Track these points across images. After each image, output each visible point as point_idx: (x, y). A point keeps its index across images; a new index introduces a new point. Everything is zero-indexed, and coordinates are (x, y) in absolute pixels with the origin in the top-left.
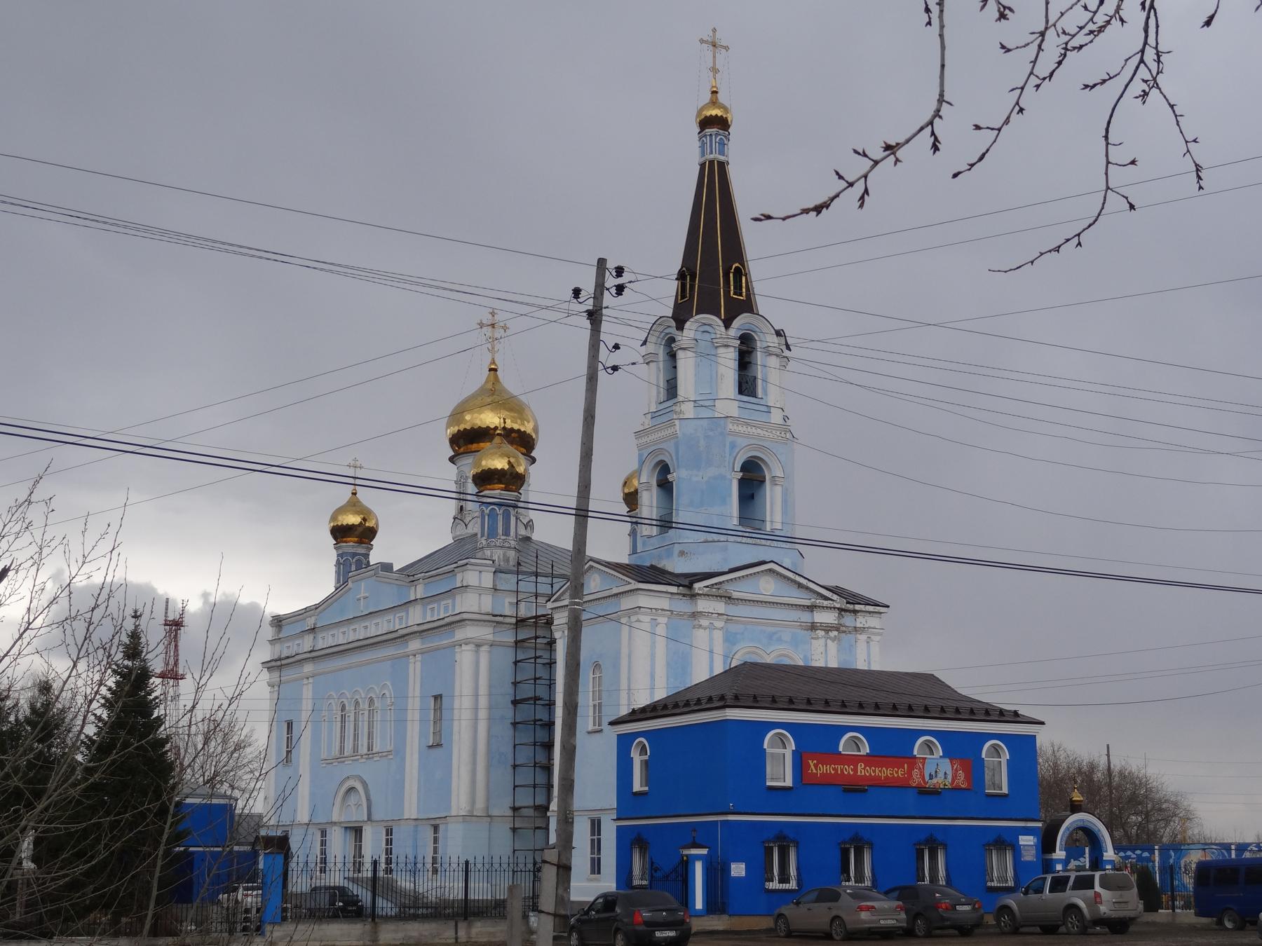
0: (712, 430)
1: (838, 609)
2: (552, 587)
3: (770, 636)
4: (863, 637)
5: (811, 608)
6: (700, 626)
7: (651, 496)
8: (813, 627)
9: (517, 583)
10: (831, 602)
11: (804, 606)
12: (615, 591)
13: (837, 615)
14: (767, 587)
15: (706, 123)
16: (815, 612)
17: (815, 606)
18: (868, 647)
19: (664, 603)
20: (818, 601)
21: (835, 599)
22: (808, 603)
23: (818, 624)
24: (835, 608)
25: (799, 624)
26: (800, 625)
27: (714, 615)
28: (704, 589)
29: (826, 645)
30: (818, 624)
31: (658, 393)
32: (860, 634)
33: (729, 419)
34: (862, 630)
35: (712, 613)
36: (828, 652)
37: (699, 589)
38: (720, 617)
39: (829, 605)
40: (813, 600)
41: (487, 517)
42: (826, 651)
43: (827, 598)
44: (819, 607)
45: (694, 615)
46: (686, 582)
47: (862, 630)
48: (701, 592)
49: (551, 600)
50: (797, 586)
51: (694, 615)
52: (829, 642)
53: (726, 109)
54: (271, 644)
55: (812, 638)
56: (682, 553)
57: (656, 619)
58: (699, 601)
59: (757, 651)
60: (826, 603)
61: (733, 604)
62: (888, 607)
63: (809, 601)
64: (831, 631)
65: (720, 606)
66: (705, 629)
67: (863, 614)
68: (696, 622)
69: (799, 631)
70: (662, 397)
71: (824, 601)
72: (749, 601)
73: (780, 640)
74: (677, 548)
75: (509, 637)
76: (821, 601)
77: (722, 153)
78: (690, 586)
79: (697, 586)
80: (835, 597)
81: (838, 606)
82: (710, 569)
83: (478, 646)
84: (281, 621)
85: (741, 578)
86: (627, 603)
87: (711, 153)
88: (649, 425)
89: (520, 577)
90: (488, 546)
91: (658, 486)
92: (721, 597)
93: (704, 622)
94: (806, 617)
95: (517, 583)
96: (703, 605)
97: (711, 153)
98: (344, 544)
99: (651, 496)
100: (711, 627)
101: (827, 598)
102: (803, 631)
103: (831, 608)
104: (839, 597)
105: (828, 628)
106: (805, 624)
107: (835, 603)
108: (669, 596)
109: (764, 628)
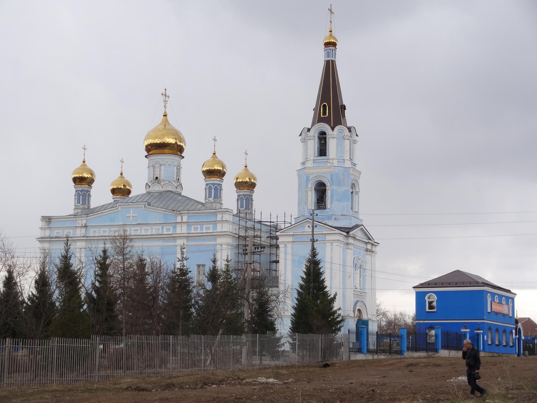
0: (345, 172)
2: (246, 223)
4: (373, 255)
6: (349, 248)
7: (312, 193)
9: (239, 221)
12: (324, 232)
15: (327, 44)
19: (341, 238)
22: (367, 241)
26: (365, 250)
31: (314, 153)
33: (352, 169)
41: (213, 190)
43: (371, 240)
45: (347, 244)
46: (346, 231)
48: (351, 236)
49: (280, 232)
51: (347, 244)
53: (336, 40)
54: (41, 230)
55: (366, 254)
56: (335, 219)
60: (370, 241)
62: (379, 244)
63: (367, 240)
68: (348, 247)
70: (316, 154)
74: (334, 217)
75: (235, 243)
77: (335, 58)
78: (348, 233)
82: (345, 226)
83: (228, 246)
84: (50, 219)
85: (325, 227)
86: (328, 238)
87: (332, 57)
88: (311, 165)
89: (240, 219)
90: (215, 202)
91: (315, 190)
93: (350, 247)
95: (239, 221)
96: (351, 241)
97: (332, 57)
98: (84, 186)
99: (312, 193)
101: (371, 240)
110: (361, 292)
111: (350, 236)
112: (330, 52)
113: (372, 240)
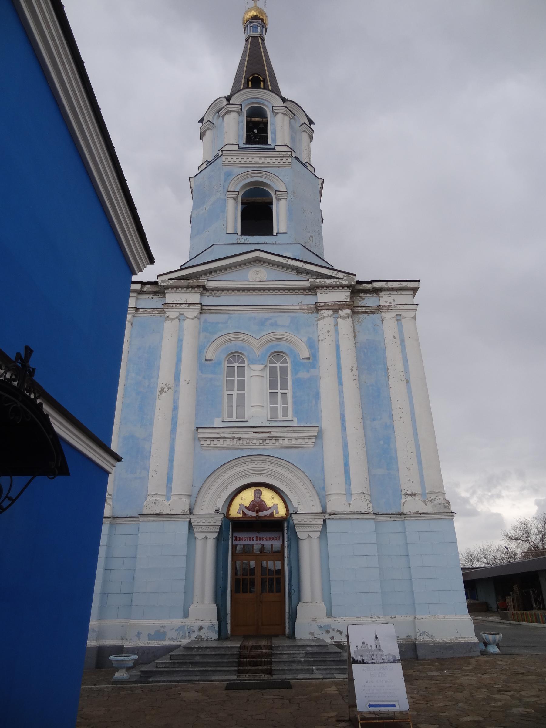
1: (348, 287)
3: (262, 323)
4: (391, 315)
5: (313, 289)
8: (317, 308)
11: (304, 289)
13: (348, 294)
16: (318, 294)
20: (318, 281)
21: (342, 277)
22: (306, 284)
23: (321, 304)
24: (343, 287)
25: (299, 307)
26: (301, 309)
28: (170, 281)
29: (336, 325)
30: (321, 304)
32: (386, 312)
34: (389, 308)
36: (340, 330)
37: (163, 281)
38: (192, 307)
39: (333, 283)
42: (337, 331)
44: (322, 287)
47: (389, 308)
48: (165, 284)
52: (340, 321)
58: (167, 294)
59: (239, 336)
60: (328, 282)
61: (213, 296)
64: (341, 309)
65: (194, 297)
66: (173, 319)
67: (387, 293)
69: (302, 314)
71: (326, 280)
73: (275, 325)
76: (322, 280)
80: (341, 275)
92: (193, 288)
94: (309, 300)
102: (306, 315)
103: (338, 287)
104: (346, 275)
105: (336, 307)
106: (306, 307)
107: (341, 281)
109: (253, 315)
111: (167, 288)
113: (341, 275)
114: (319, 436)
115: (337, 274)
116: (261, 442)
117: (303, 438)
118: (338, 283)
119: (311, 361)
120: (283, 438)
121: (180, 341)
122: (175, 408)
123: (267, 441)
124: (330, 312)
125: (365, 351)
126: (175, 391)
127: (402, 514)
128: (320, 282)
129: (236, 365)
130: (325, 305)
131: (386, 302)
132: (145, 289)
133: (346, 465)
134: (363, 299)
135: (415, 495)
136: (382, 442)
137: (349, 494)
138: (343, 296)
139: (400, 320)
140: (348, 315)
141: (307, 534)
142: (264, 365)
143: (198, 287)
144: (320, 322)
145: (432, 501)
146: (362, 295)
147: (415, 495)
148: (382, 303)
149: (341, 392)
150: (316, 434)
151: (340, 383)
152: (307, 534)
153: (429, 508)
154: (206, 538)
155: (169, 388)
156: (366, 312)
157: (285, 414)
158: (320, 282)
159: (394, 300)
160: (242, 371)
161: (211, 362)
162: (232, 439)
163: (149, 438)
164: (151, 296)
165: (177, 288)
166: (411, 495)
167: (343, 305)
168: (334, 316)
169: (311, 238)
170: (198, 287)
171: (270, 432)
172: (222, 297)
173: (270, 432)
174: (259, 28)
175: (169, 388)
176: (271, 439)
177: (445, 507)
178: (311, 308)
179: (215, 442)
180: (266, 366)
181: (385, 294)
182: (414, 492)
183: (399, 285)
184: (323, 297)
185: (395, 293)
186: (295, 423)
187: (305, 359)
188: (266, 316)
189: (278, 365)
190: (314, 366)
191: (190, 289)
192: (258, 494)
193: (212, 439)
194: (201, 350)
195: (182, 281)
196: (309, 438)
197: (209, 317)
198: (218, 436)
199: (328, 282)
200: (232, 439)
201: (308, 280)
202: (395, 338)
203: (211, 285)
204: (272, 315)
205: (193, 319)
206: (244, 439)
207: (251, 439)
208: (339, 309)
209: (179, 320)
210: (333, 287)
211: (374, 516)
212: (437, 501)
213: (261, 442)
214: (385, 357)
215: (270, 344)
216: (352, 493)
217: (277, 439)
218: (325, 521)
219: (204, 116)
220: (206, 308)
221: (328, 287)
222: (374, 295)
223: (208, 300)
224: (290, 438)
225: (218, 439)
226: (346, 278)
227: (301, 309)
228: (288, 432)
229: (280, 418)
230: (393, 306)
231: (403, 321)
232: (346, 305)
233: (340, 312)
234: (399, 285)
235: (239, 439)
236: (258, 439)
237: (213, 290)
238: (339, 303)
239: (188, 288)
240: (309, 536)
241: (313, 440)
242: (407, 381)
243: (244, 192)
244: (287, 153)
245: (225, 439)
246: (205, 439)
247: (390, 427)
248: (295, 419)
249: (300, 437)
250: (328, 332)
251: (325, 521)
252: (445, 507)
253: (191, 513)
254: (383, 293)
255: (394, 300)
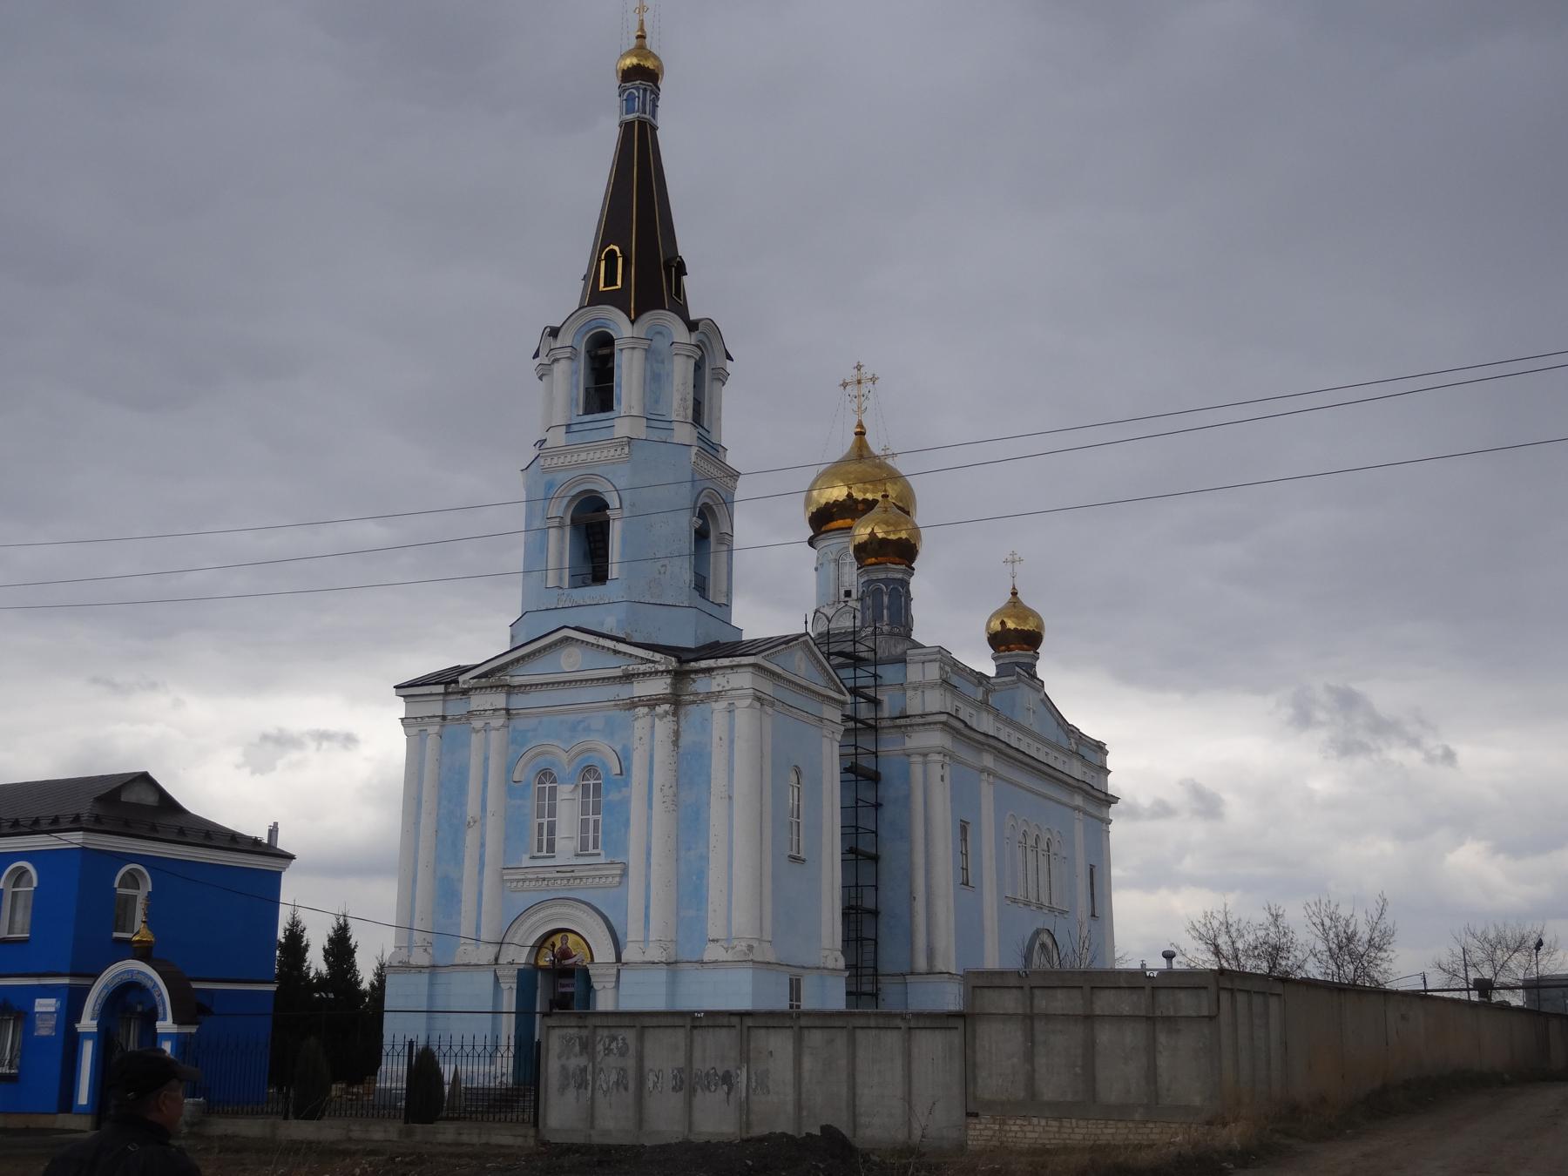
1: (668, 672)
4: (720, 706)
5: (628, 678)
8: (633, 704)
10: (651, 665)
13: (669, 681)
14: (570, 662)
17: (633, 675)
18: (732, 719)
20: (630, 668)
21: (658, 659)
22: (618, 673)
23: (637, 699)
25: (613, 703)
26: (616, 705)
27: (488, 712)
29: (653, 727)
32: (716, 701)
35: (486, 710)
37: (464, 682)
38: (497, 713)
39: (649, 670)
40: (625, 667)
42: (652, 735)
44: (639, 674)
48: (466, 686)
50: (611, 652)
57: (426, 730)
59: (544, 749)
61: (523, 693)
64: (659, 705)
65: (499, 700)
66: (478, 731)
67: (720, 672)
72: (542, 684)
76: (635, 667)
79: (461, 679)
80: (657, 657)
81: (662, 668)
92: (497, 687)
93: (477, 723)
100: (486, 728)
104: (663, 656)
105: (652, 703)
107: (657, 666)
108: (441, 697)
110: (558, 869)
111: (470, 689)
112: (637, 94)
114: (624, 873)
115: (653, 656)
116: (565, 882)
117: (607, 877)
118: (653, 670)
119: (624, 777)
120: (588, 877)
121: (486, 759)
122: (483, 845)
123: (572, 881)
124: (646, 710)
125: (689, 757)
126: (482, 825)
127: (702, 962)
128: (633, 669)
129: (547, 785)
130: (639, 701)
131: (719, 685)
132: (450, 690)
133: (647, 907)
134: (694, 681)
135: (717, 941)
136: (694, 878)
137: (646, 941)
138: (660, 686)
139: (733, 710)
140: (666, 713)
141: (602, 985)
142: (573, 786)
143: (503, 686)
144: (636, 723)
145: (733, 948)
146: (692, 676)
147: (717, 941)
148: (715, 689)
149: (649, 818)
150: (619, 872)
151: (650, 806)
152: (602, 985)
153: (729, 957)
154: (511, 987)
155: (475, 822)
156: (694, 702)
157: (595, 847)
158: (633, 669)
159: (728, 682)
160: (553, 791)
161: (519, 784)
162: (537, 880)
163: (460, 880)
164: (459, 697)
165: (481, 688)
166: (713, 941)
167: (660, 699)
168: (652, 714)
169: (662, 570)
170: (503, 686)
171: (573, 871)
172: (532, 694)
173: (573, 871)
174: (637, 99)
175: (475, 822)
176: (575, 878)
177: (745, 954)
178: (627, 704)
179: (521, 883)
180: (577, 786)
181: (718, 674)
182: (716, 937)
183: (731, 661)
184: (642, 689)
185: (729, 671)
186: (602, 860)
187: (617, 774)
188: (580, 717)
189: (592, 782)
190: (627, 784)
191: (495, 689)
192: (565, 939)
193: (518, 881)
194: (509, 770)
195: (483, 680)
196: (613, 876)
197: (518, 723)
198: (523, 877)
199: (643, 668)
200: (537, 880)
201: (620, 667)
202: (721, 739)
203: (517, 681)
204: (586, 715)
205: (498, 730)
206: (549, 879)
207: (555, 879)
208: (656, 704)
209: (485, 730)
210: (651, 673)
211: (665, 966)
212: (738, 948)
213: (565, 882)
214: (710, 766)
215: (581, 757)
216: (650, 939)
217: (581, 878)
218: (619, 970)
219: (539, 348)
220: (514, 712)
221: (644, 674)
222: (707, 675)
223: (518, 701)
224: (594, 877)
225: (524, 880)
226: (663, 660)
227: (616, 705)
228: (590, 870)
229: (591, 851)
230: (723, 693)
231: (736, 711)
232: (664, 699)
233: (657, 708)
234: (731, 661)
235: (544, 879)
236: (562, 879)
237: (520, 686)
238: (655, 697)
239: (491, 687)
240: (604, 987)
241: (617, 879)
242: (730, 798)
243: (573, 508)
244: (621, 440)
245: (531, 880)
246: (512, 881)
247: (704, 858)
248: (603, 853)
249: (603, 876)
250: (641, 738)
251: (619, 970)
252: (745, 954)
253: (496, 964)
254: (715, 673)
255: (728, 682)
